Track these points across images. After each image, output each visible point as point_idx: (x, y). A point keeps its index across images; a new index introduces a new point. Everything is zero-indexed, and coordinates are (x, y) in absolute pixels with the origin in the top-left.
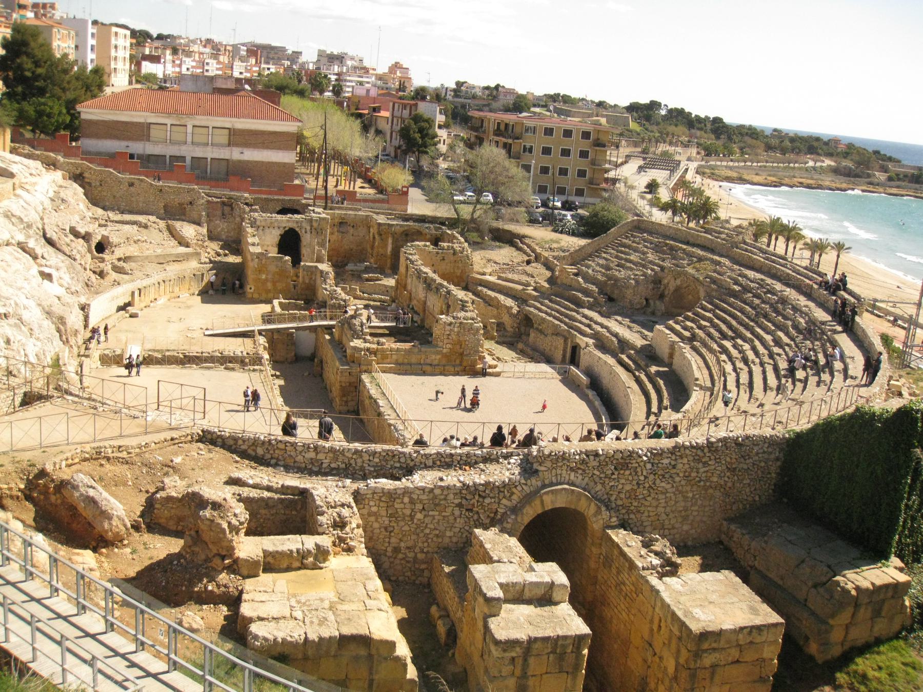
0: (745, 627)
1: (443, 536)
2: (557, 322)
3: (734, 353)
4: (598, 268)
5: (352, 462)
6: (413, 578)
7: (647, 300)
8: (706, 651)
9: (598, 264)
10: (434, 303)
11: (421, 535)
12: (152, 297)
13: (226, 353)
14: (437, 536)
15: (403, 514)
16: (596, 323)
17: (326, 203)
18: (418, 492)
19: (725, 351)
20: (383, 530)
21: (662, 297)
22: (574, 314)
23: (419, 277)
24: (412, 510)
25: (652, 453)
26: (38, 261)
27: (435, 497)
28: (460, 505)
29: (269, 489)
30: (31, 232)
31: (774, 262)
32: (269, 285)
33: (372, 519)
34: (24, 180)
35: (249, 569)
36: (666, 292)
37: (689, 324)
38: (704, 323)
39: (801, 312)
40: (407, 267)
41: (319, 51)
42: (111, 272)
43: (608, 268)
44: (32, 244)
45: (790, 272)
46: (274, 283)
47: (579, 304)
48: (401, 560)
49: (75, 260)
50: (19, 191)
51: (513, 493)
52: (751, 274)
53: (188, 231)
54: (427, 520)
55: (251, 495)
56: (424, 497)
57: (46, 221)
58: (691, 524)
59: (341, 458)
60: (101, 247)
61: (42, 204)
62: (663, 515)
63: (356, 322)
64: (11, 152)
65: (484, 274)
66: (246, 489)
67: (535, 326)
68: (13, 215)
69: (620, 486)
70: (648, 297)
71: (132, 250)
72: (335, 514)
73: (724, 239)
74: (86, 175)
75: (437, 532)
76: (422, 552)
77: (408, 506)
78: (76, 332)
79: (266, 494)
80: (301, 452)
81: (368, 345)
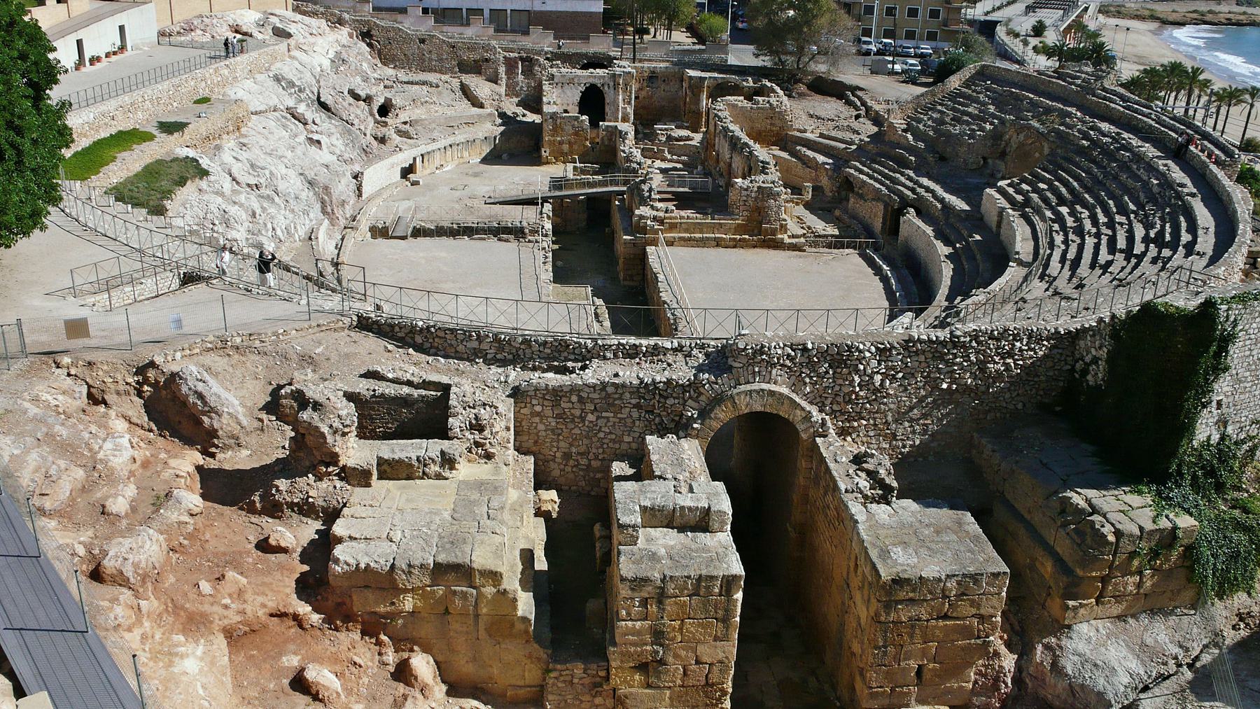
0: (954, 576)
1: (621, 442)
2: (878, 186)
3: (1070, 222)
4: (930, 123)
5: (521, 352)
6: (588, 488)
7: (985, 159)
8: (901, 602)
9: (931, 118)
10: (738, 163)
11: (595, 439)
12: (437, 163)
13: (503, 224)
14: (613, 441)
15: (572, 415)
16: (921, 186)
17: (634, 56)
18: (587, 389)
19: (1060, 219)
20: (549, 432)
21: (1003, 155)
22: (898, 175)
23: (725, 136)
24: (582, 410)
25: (877, 348)
26: (307, 126)
27: (608, 395)
28: (638, 406)
29: (409, 383)
30: (303, 96)
31: (1136, 111)
32: (566, 147)
33: (537, 419)
34: (302, 40)
35: (359, 477)
36: (1008, 150)
37: (1025, 186)
38: (1042, 186)
39: (1157, 170)
40: (716, 125)
42: (394, 136)
43: (944, 123)
44: (302, 109)
45: (1153, 123)
47: (902, 163)
48: (572, 467)
49: (352, 124)
50: (295, 53)
51: (700, 394)
52: (1105, 126)
53: (482, 88)
55: (387, 391)
56: (596, 396)
57: (322, 84)
59: (507, 348)
60: (384, 110)
61: (320, 66)
63: (645, 187)
66: (384, 384)
67: (856, 189)
69: (837, 388)
70: (986, 155)
71: (418, 113)
72: (472, 416)
73: (1077, 86)
74: (373, 32)
75: (613, 437)
76: (596, 458)
77: (577, 405)
78: (343, 203)
79: (406, 390)
80: (462, 341)
81: (655, 213)
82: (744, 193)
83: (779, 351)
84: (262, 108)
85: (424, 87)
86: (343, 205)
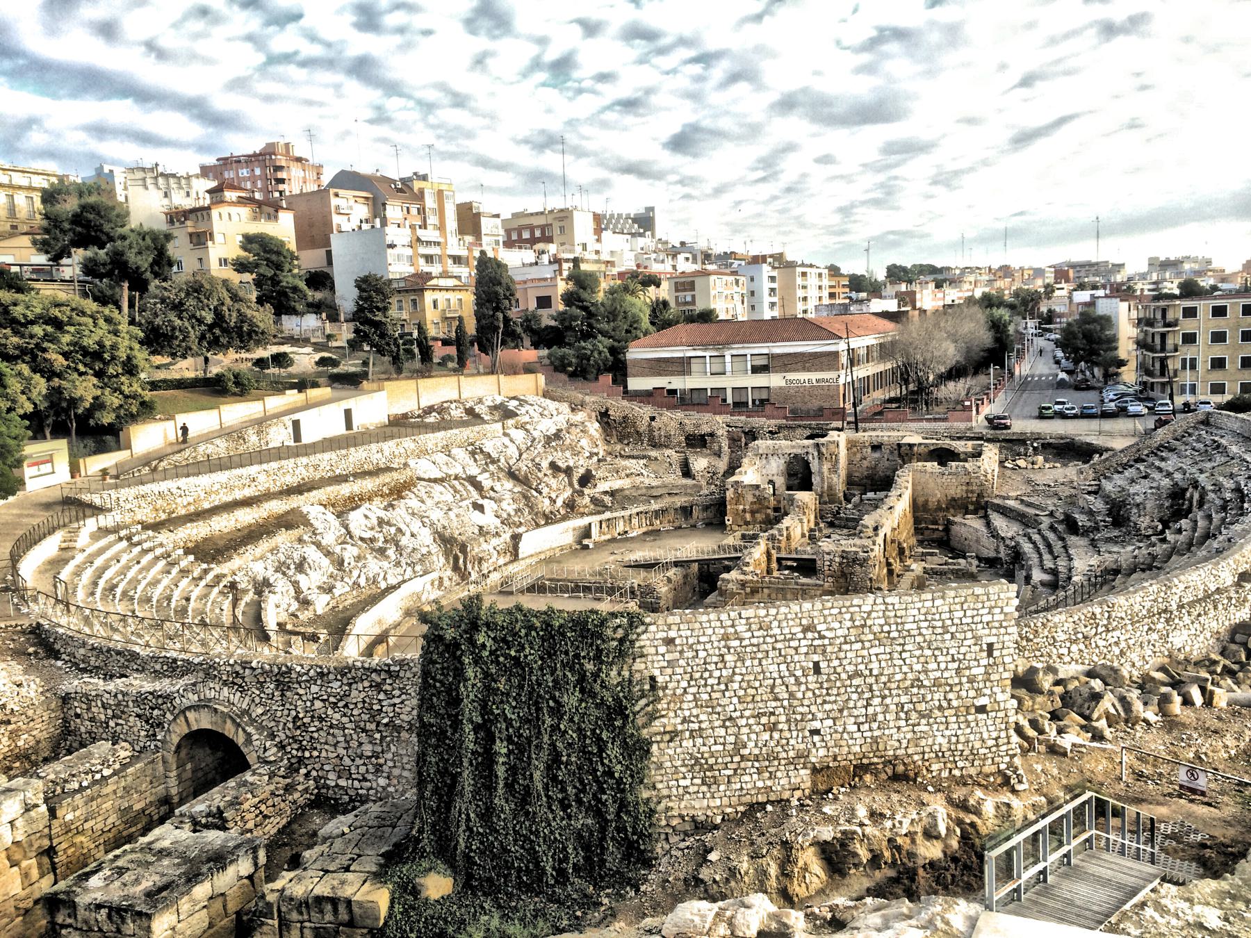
32: (748, 516)
41: (1150, 259)
46: (753, 512)
49: (540, 493)
54: (119, 728)
58: (388, 778)
60: (586, 479)
62: (346, 758)
64: (544, 396)
65: (1008, 498)
68: (482, 451)
74: (610, 412)
82: (827, 557)
83: (229, 669)
84: (439, 475)
85: (642, 462)
86: (480, 563)
